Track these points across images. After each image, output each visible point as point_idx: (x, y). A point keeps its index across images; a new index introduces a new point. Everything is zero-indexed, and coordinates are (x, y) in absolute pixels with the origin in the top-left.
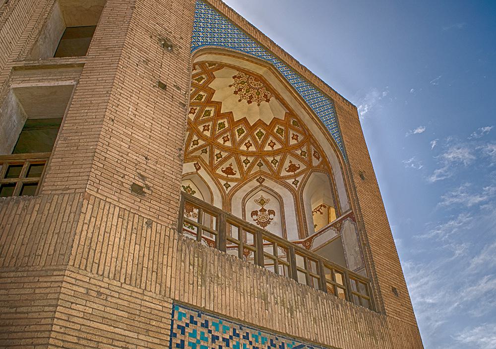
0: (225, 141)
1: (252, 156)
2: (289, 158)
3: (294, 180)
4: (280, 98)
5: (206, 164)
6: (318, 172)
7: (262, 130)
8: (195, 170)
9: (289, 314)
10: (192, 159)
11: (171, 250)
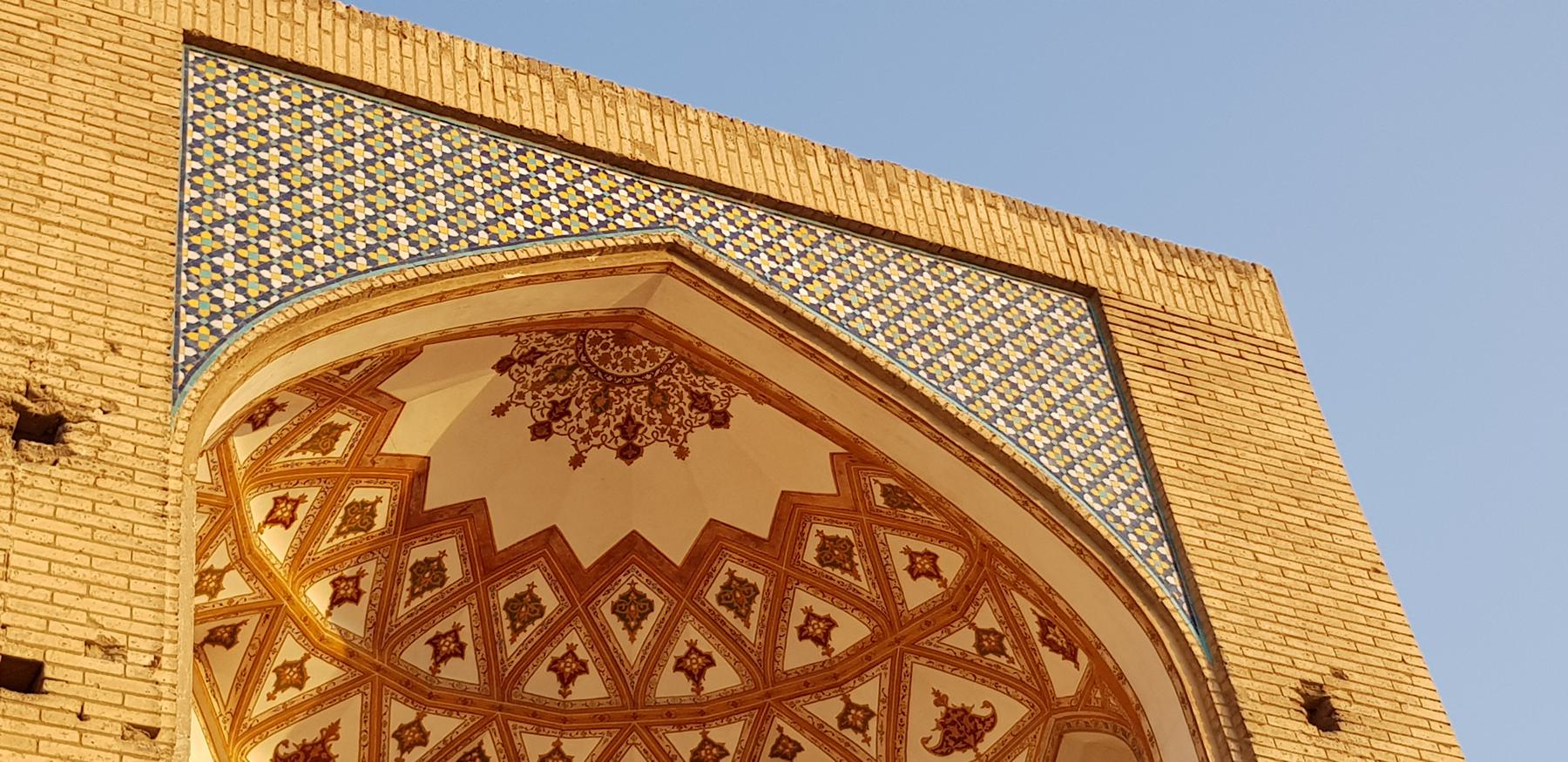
1: (727, 719)
2: (925, 680)
4: (775, 395)
6: (1087, 728)
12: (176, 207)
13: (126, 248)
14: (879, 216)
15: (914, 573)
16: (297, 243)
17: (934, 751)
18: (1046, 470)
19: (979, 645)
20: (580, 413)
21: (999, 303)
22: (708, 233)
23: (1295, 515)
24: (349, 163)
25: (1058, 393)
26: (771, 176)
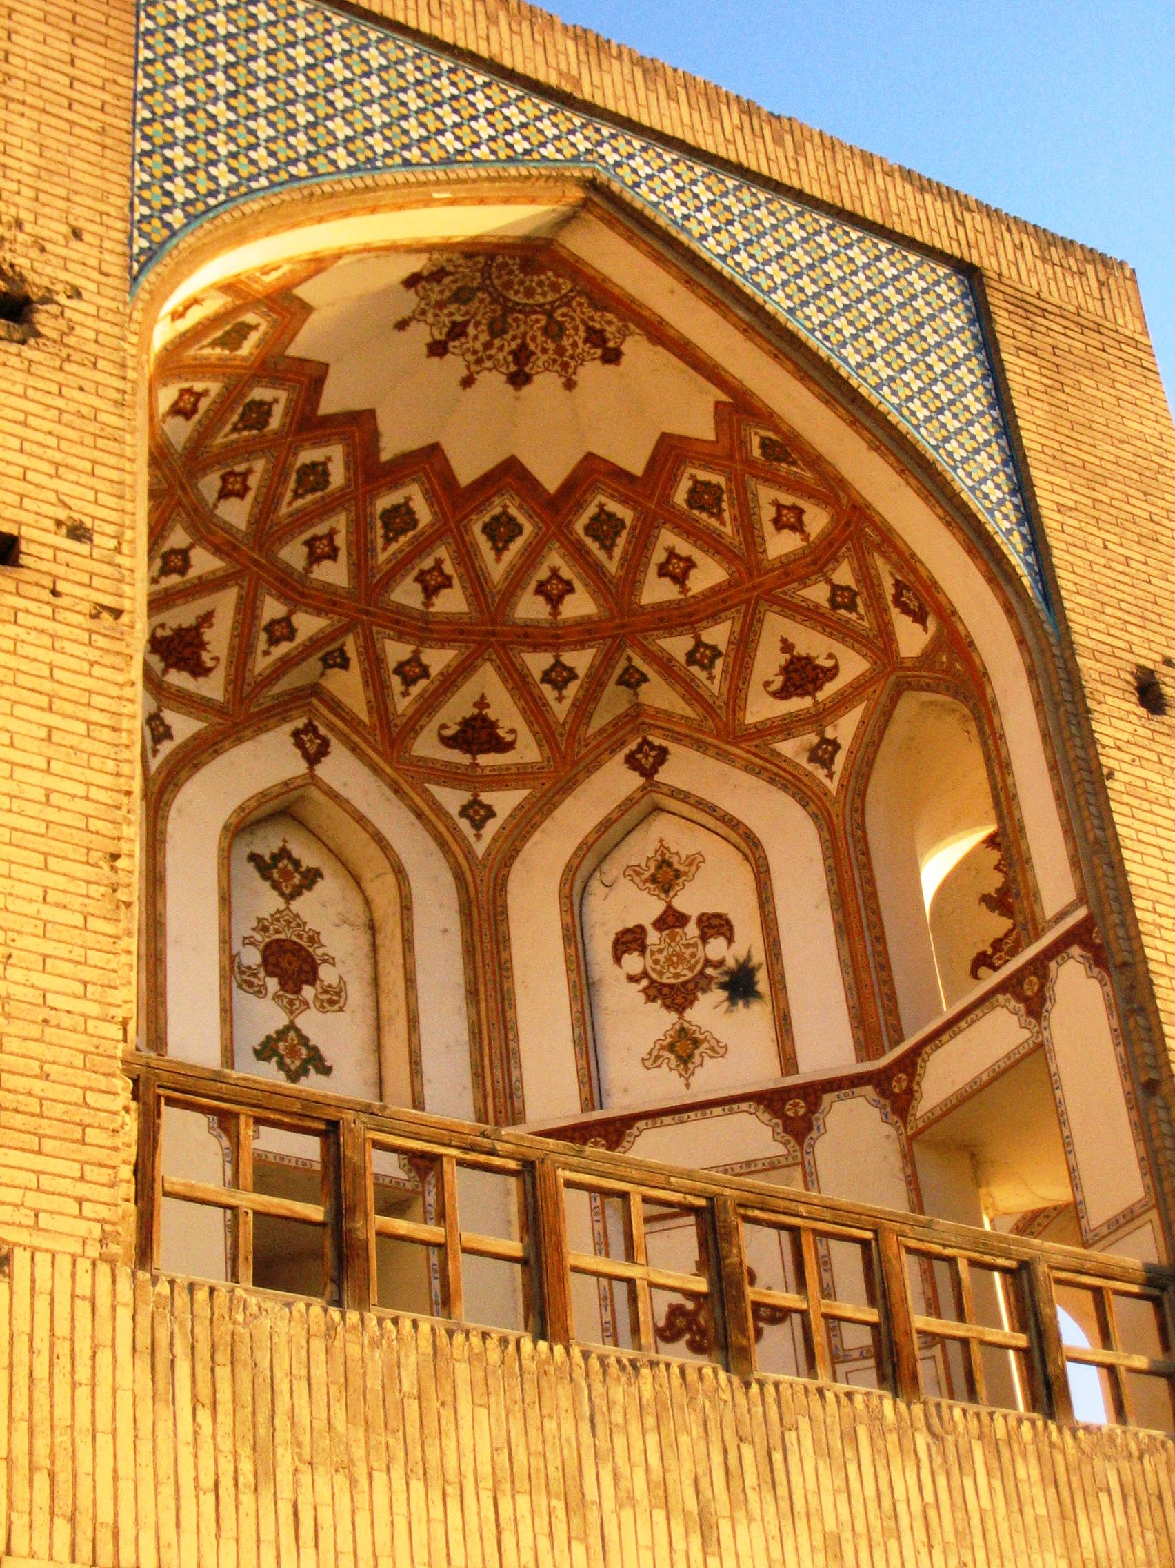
0: (430, 592)
1: (581, 645)
3: (813, 739)
5: (351, 720)
7: (613, 507)
8: (301, 767)
9: (696, 1540)
10: (278, 712)
11: (104, 1357)
12: (131, 95)
13: (86, 133)
14: (785, 173)
15: (779, 524)
16: (243, 143)
17: (775, 694)
18: (925, 439)
19: (832, 600)
20: (477, 335)
21: (890, 272)
22: (625, 172)
23: (1140, 509)
24: (292, 67)
25: (939, 367)
26: (687, 120)
